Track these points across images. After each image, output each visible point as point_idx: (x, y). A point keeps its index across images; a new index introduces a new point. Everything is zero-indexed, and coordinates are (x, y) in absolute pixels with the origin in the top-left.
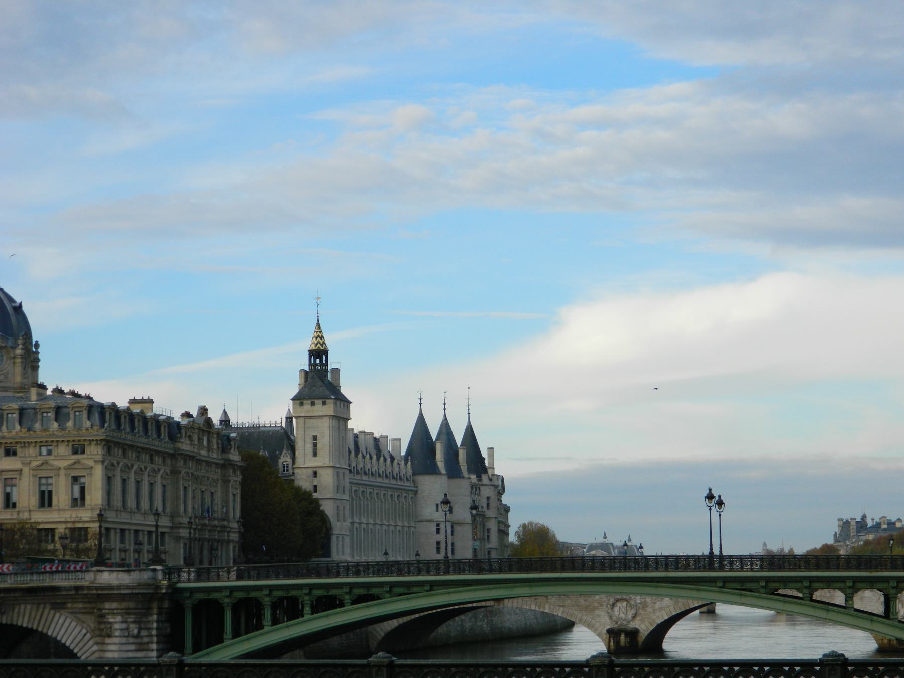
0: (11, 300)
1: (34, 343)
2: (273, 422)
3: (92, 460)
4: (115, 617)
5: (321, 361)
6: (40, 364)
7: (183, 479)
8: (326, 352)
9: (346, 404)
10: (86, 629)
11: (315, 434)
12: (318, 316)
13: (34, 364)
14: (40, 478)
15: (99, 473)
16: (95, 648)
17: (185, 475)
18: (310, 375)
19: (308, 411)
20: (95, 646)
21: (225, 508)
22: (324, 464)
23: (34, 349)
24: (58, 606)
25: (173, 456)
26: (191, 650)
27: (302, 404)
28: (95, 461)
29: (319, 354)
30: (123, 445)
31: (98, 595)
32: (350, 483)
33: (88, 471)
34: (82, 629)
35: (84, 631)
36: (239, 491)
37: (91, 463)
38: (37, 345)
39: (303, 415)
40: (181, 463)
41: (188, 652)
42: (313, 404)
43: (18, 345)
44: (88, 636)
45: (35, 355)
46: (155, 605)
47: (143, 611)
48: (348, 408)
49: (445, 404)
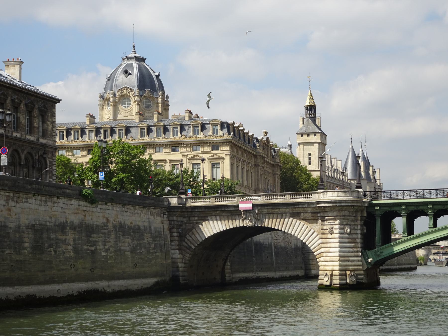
0: (154, 72)
1: (166, 96)
2: (283, 147)
3: (224, 154)
4: (335, 221)
5: (311, 112)
6: (169, 108)
7: (261, 169)
8: (315, 107)
9: (325, 136)
10: (314, 229)
11: (309, 153)
12: (310, 87)
13: (167, 108)
14: (193, 164)
15: (227, 160)
16: (320, 241)
17: (261, 167)
18: (306, 120)
19: (306, 140)
20: (320, 240)
21: (275, 190)
22: (315, 169)
23: (166, 100)
24: (295, 215)
25: (255, 156)
26: (380, 243)
27: (302, 136)
28: (226, 154)
29: (311, 109)
30: (238, 146)
31: (324, 207)
32: (327, 181)
33: (222, 160)
34: (311, 229)
35: (312, 231)
36: (279, 180)
37: (223, 155)
38: (167, 97)
39: (303, 142)
40: (259, 160)
41: (378, 244)
42: (308, 135)
43: (159, 96)
44: (315, 234)
45: (167, 103)
46: (359, 214)
47: (353, 218)
48: (326, 138)
49: (361, 142)
